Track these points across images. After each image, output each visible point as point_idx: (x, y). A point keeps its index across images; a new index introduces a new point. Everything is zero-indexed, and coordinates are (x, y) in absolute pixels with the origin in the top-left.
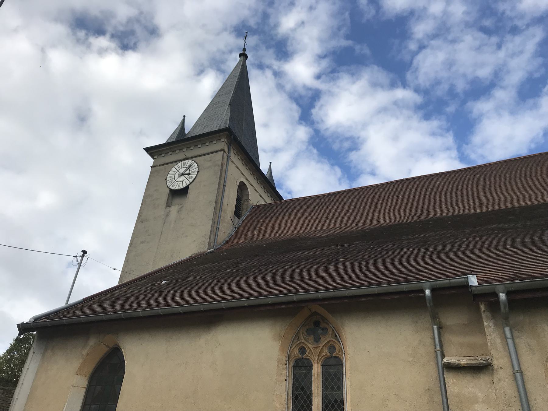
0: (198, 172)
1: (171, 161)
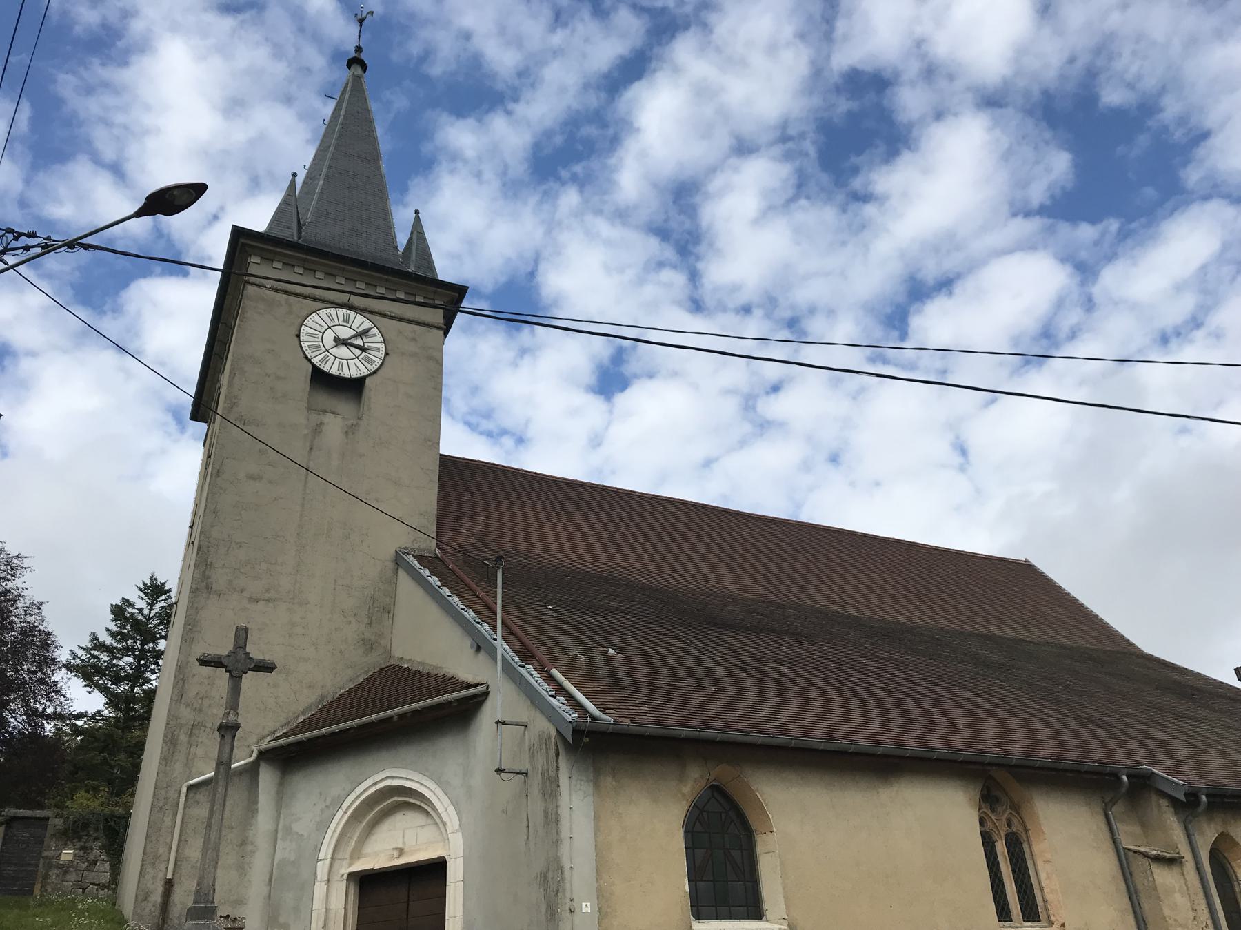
0: (387, 354)
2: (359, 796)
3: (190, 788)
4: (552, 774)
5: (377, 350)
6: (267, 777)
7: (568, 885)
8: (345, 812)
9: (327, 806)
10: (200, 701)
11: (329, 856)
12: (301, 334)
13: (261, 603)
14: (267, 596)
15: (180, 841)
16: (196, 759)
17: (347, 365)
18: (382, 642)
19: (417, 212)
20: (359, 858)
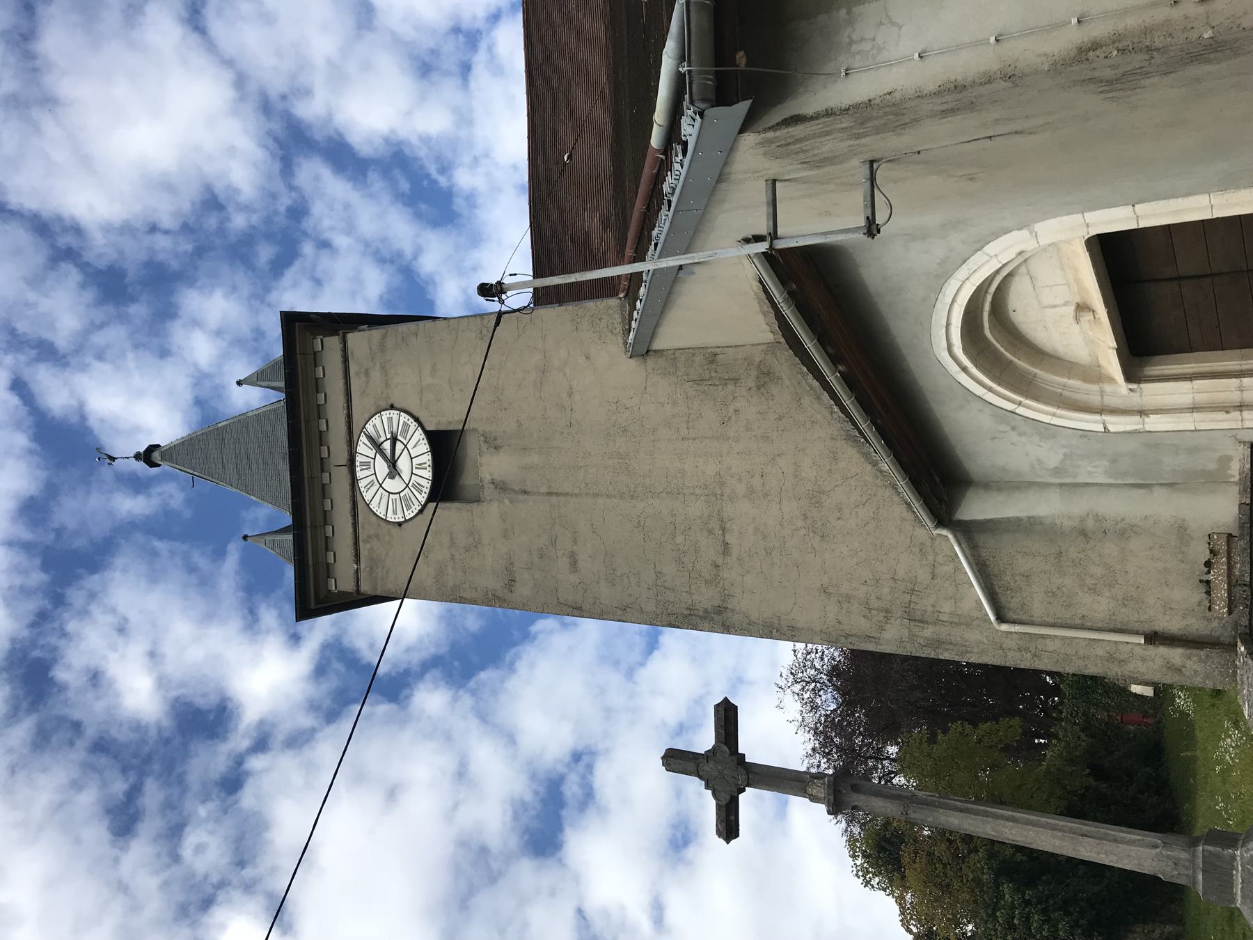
0: (392, 407)
1: (350, 520)
2: (990, 389)
3: (1001, 618)
4: (846, 122)
5: (390, 420)
6: (975, 508)
7: (1132, 22)
8: (1020, 404)
9: (1013, 428)
10: (874, 612)
11: (1097, 417)
12: (397, 520)
13: (728, 538)
14: (718, 532)
15: (1083, 628)
16: (959, 613)
18: (757, 359)
19: (239, 383)
20: (1099, 366)
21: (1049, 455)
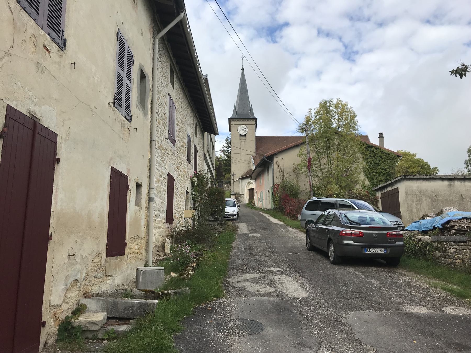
6: (240, 180)
17: (243, 133)
21: (244, 185)
